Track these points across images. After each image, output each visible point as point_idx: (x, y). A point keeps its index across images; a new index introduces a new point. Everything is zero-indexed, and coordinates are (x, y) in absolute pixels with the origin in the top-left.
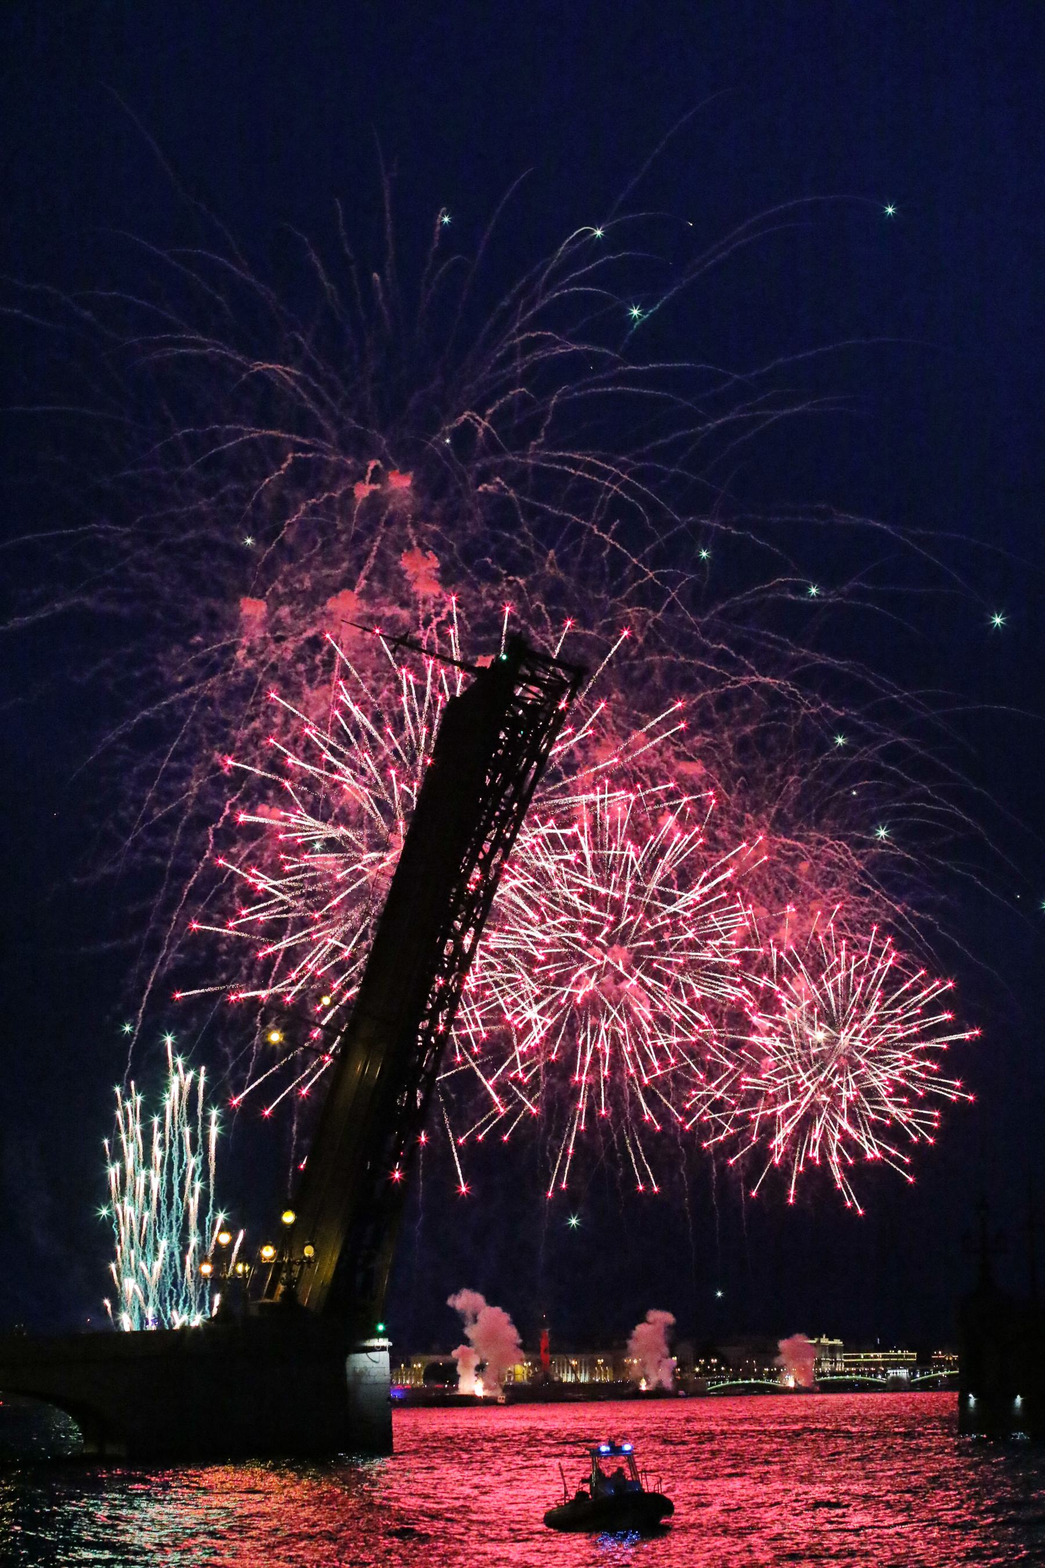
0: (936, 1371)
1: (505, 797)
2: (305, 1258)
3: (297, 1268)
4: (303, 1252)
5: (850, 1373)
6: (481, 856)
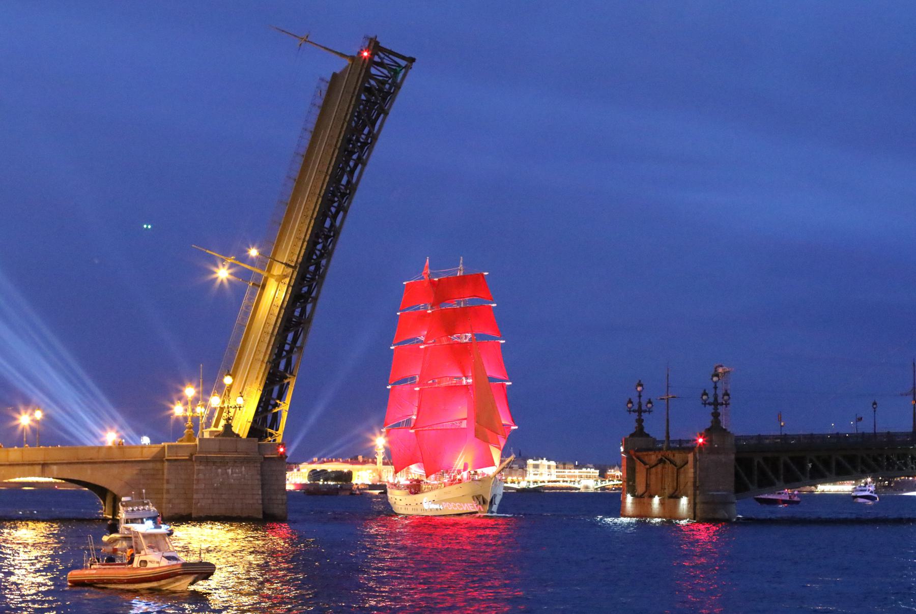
0: (609, 481)
2: (238, 405)
3: (232, 411)
4: (235, 400)
5: (559, 481)
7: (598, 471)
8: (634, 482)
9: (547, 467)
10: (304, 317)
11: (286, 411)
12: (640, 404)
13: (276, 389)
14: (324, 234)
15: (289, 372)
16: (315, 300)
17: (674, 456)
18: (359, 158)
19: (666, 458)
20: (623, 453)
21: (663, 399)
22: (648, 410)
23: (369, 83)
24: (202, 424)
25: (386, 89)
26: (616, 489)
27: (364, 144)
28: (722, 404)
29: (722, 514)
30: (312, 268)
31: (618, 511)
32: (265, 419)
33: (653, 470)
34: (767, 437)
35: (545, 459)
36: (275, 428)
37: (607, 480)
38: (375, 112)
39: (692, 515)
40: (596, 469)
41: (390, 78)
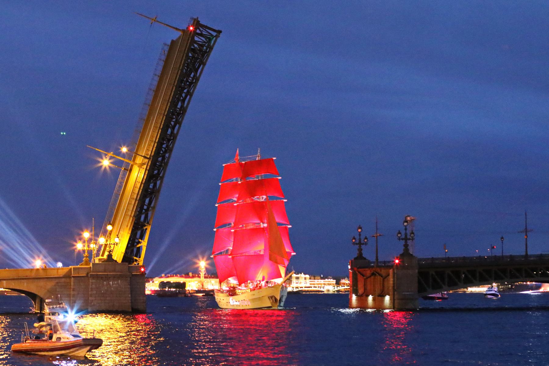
0: (342, 286)
1: (191, 77)
2: (115, 242)
3: (112, 246)
4: (114, 240)
5: (311, 287)
6: (182, 98)
7: (335, 281)
8: (357, 287)
9: (304, 278)
10: (155, 189)
11: (145, 246)
12: (360, 240)
13: (139, 233)
14: (167, 138)
15: (146, 223)
16: (162, 178)
17: (381, 271)
18: (188, 92)
19: (376, 272)
20: (350, 269)
21: (374, 236)
22: (365, 243)
23: (194, 46)
24: (94, 254)
25: (204, 50)
26: (346, 291)
27: (191, 83)
28: (410, 239)
29: (410, 306)
30: (160, 159)
31: (348, 305)
32: (132, 251)
33: (369, 279)
34: (437, 259)
35: (303, 273)
36: (138, 257)
37: (341, 286)
38: (197, 64)
39: (392, 307)
40: (334, 279)
41: (206, 43)
